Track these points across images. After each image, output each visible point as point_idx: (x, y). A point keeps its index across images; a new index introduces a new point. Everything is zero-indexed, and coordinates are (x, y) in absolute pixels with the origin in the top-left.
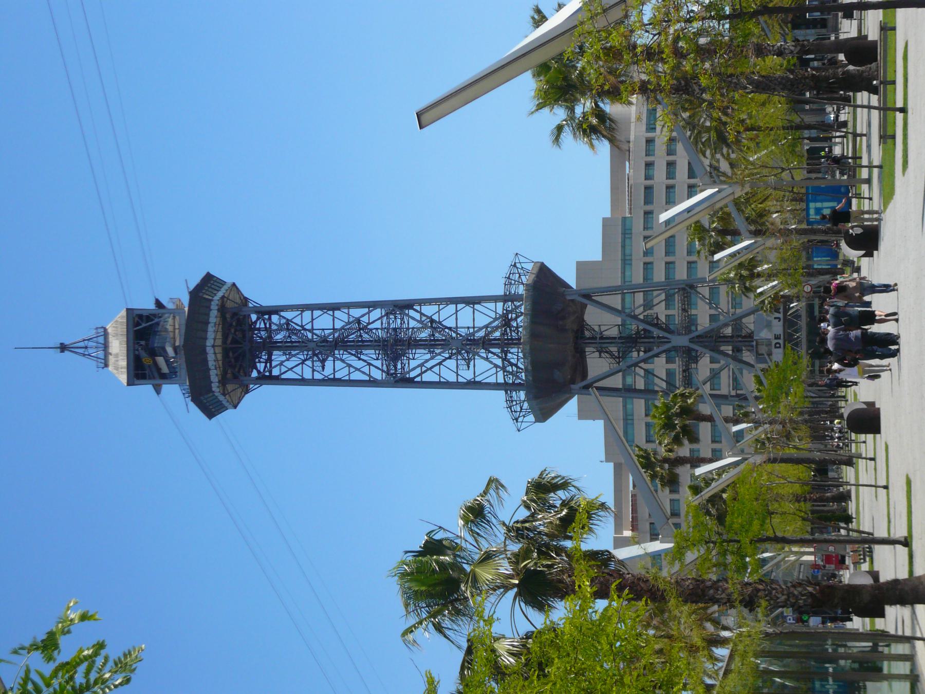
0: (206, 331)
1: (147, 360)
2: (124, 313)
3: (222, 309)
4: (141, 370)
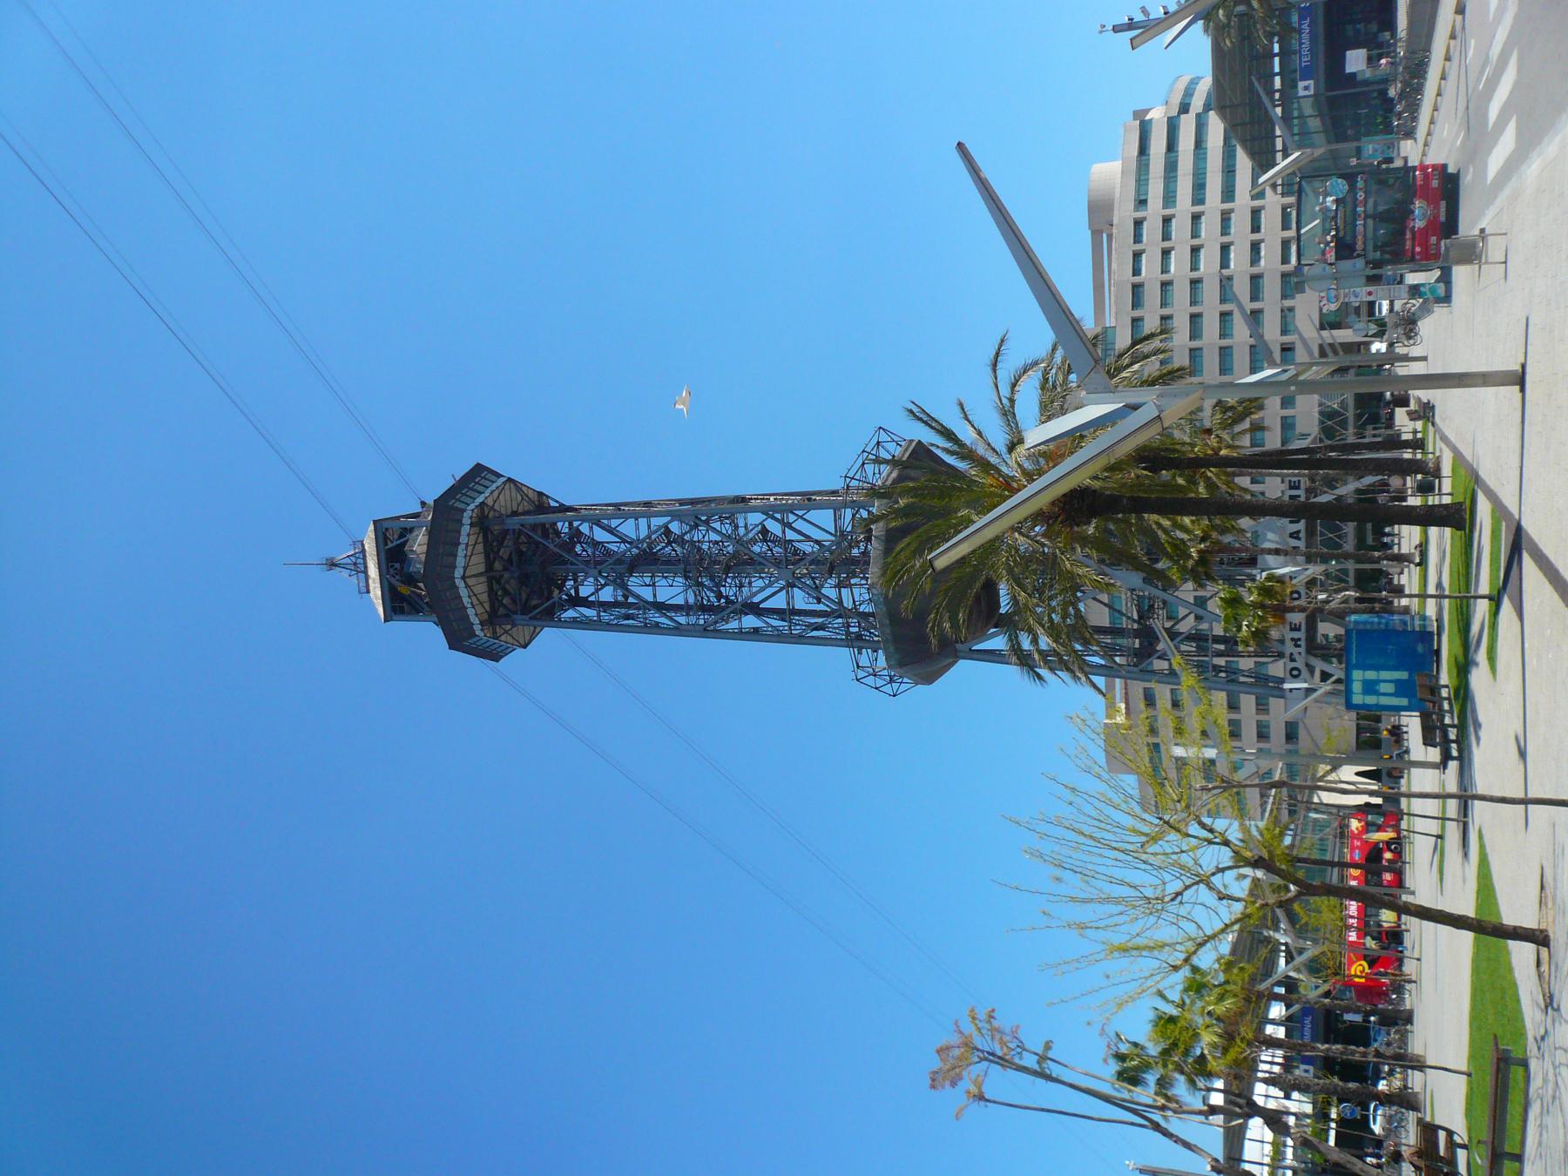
0: (455, 556)
1: (404, 590)
2: (372, 527)
3: (482, 522)
4: (399, 605)
